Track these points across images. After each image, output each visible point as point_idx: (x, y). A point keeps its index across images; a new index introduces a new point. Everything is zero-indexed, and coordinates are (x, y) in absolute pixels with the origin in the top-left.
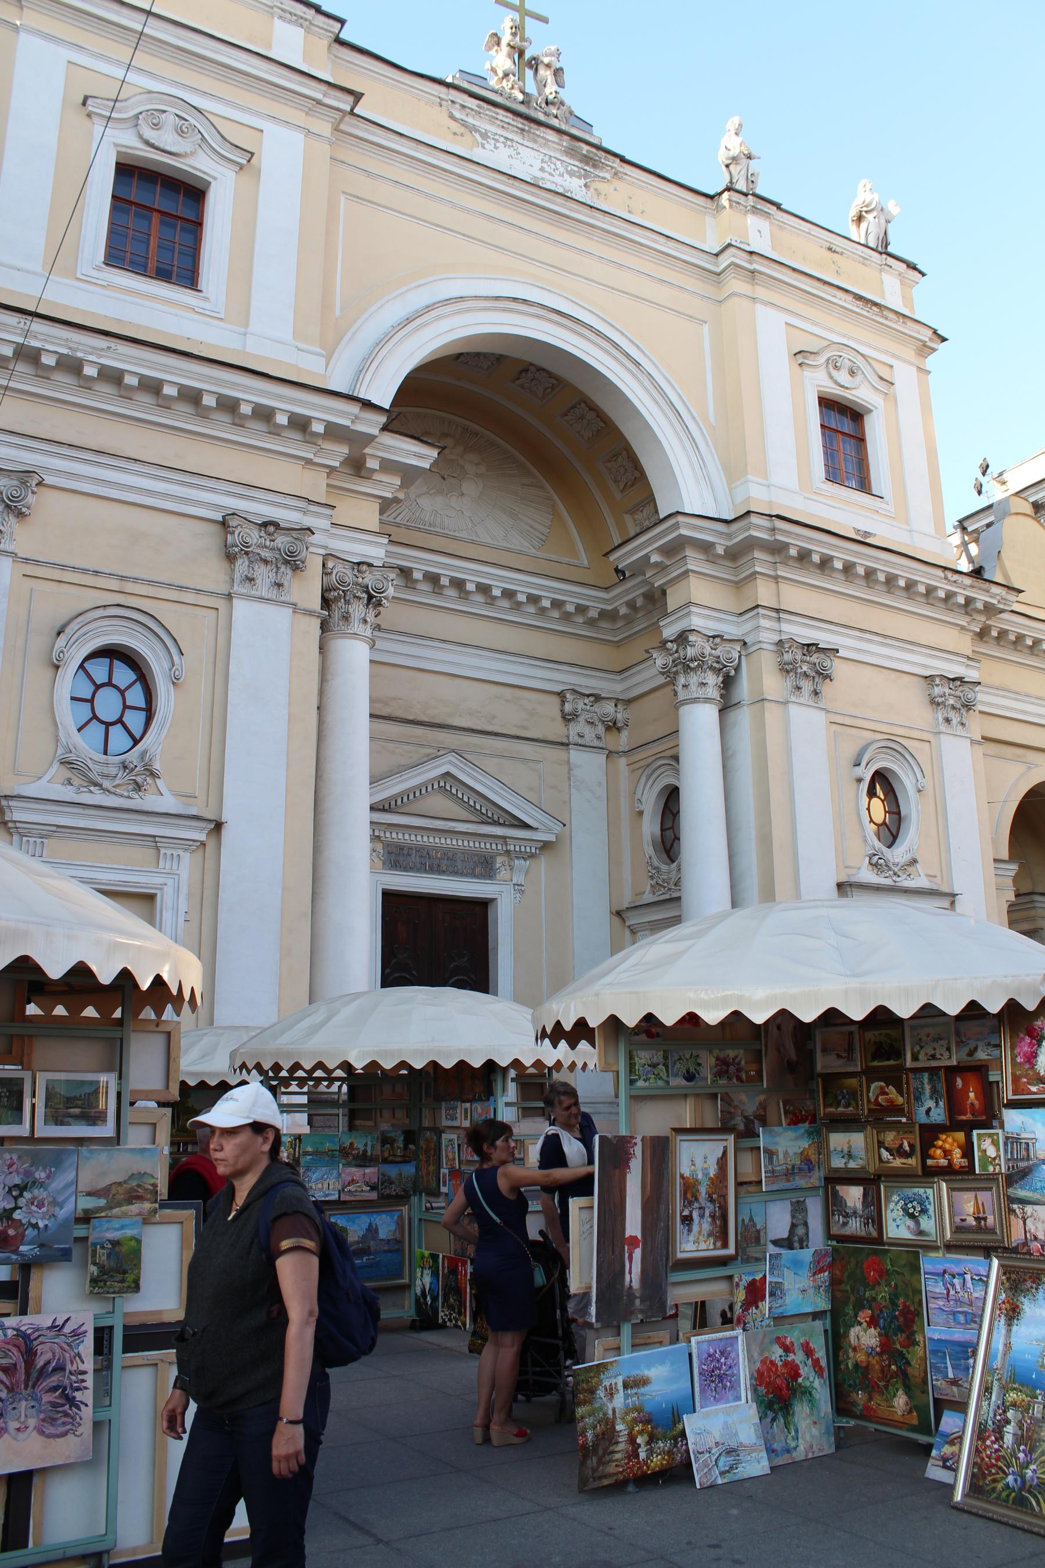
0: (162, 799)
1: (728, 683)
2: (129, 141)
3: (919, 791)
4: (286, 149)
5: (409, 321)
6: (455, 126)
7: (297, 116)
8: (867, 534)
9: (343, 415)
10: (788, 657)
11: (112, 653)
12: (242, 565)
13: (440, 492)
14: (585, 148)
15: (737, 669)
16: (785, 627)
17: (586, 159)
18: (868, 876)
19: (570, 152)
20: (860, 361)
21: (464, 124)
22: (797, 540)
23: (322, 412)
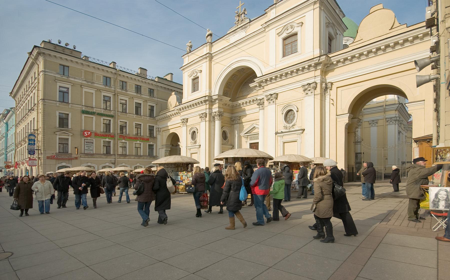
3: (297, 111)
7: (205, 60)
23: (204, 99)
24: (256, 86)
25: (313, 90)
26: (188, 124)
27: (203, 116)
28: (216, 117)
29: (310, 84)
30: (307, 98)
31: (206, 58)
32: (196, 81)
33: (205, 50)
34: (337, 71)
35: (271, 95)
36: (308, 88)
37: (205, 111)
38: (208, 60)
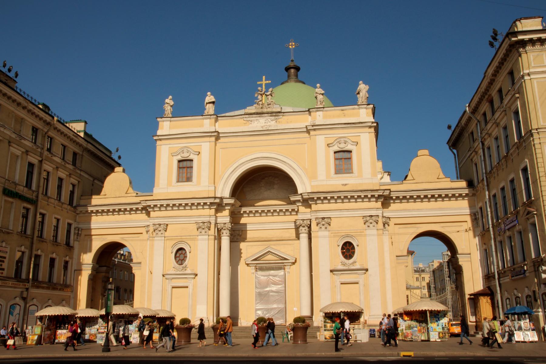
0: (189, 271)
1: (310, 227)
2: (179, 157)
4: (206, 146)
5: (233, 171)
6: (245, 122)
8: (346, 185)
9: (212, 200)
10: (317, 221)
11: (181, 249)
12: (200, 230)
13: (269, 189)
14: (274, 114)
15: (310, 225)
16: (318, 214)
17: (275, 116)
18: (341, 267)
19: (271, 116)
20: (347, 140)
21: (247, 121)
22: (315, 196)
23: (208, 201)
24: (299, 201)
25: (374, 224)
26: (167, 234)
27: (203, 227)
28: (224, 232)
29: (372, 216)
30: (368, 232)
31: (211, 136)
32: (185, 164)
33: (206, 124)
34: (394, 206)
35: (323, 218)
36: (370, 220)
37: (208, 219)
38: (213, 139)
